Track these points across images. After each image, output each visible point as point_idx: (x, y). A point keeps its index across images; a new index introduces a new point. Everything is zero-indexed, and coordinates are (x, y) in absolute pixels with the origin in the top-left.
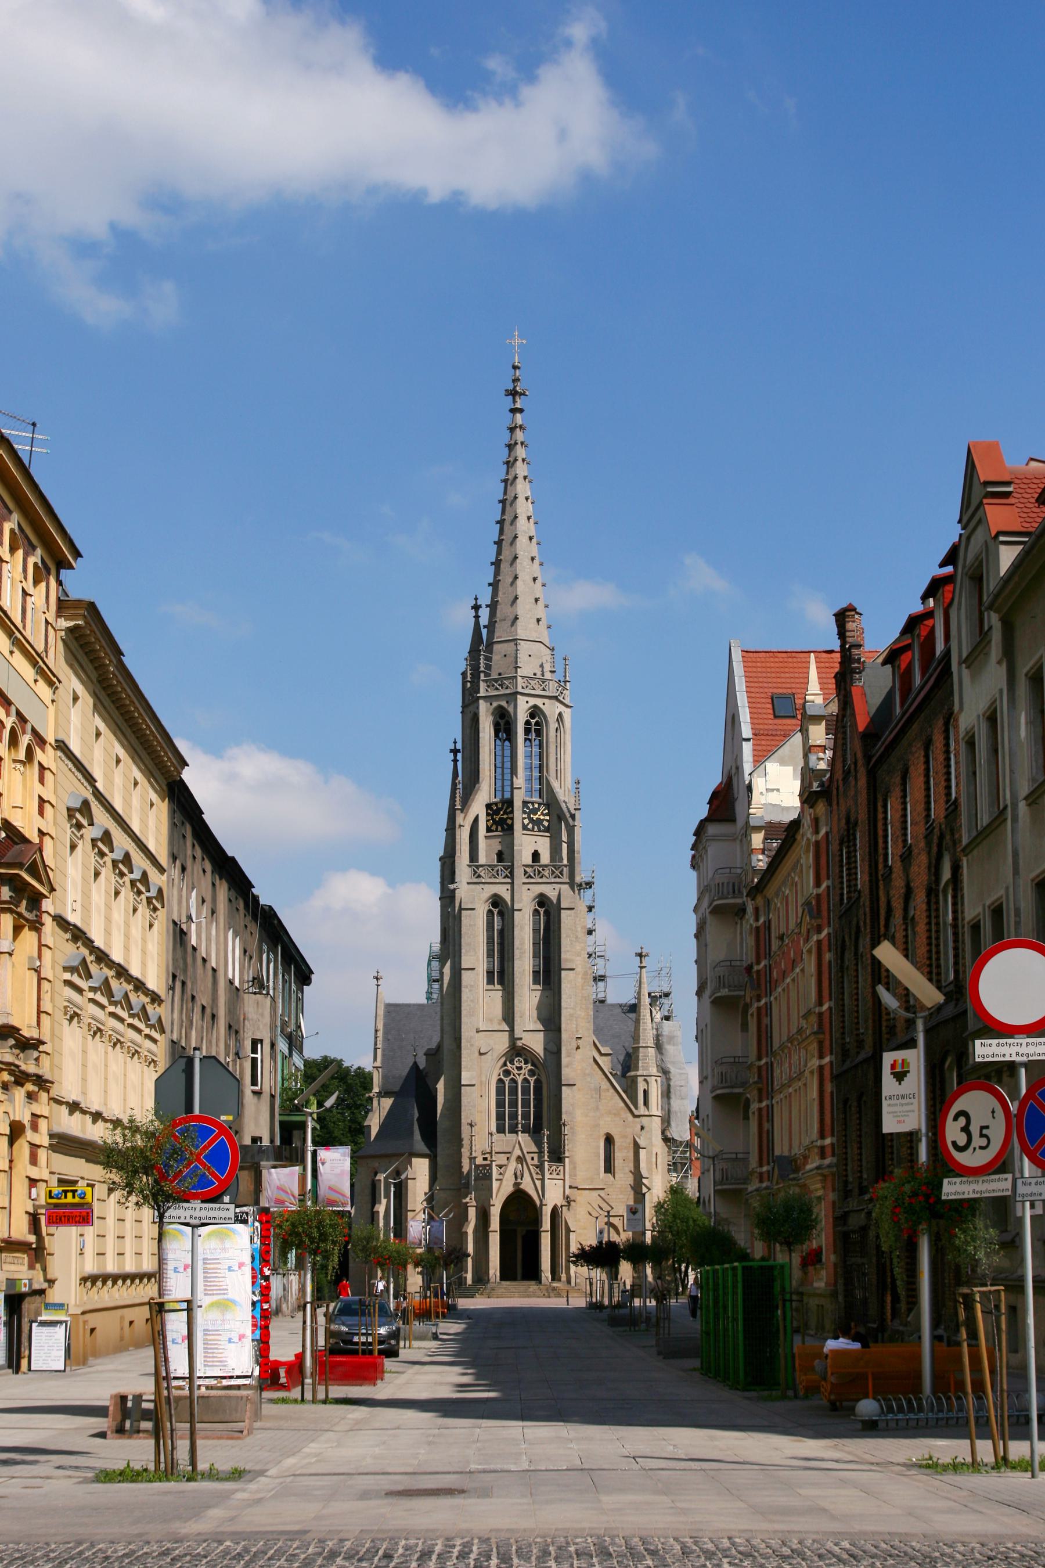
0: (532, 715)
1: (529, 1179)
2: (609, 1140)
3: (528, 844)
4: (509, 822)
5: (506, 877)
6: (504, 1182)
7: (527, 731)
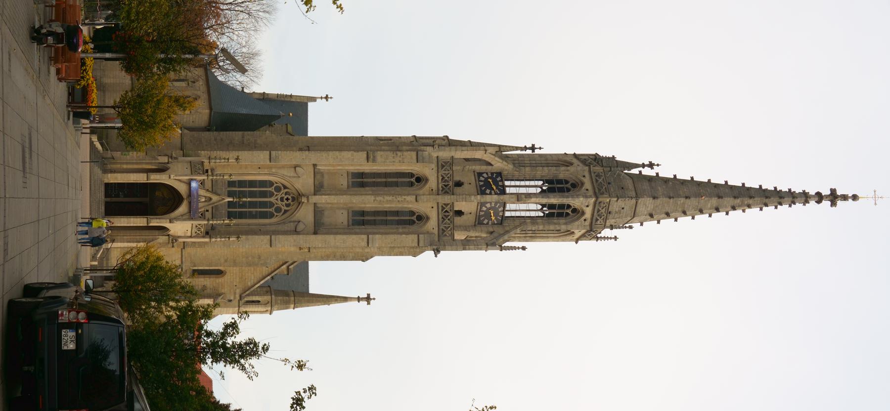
0: (575, 211)
2: (219, 273)
3: (468, 205)
4: (488, 191)
5: (443, 189)
7: (562, 206)
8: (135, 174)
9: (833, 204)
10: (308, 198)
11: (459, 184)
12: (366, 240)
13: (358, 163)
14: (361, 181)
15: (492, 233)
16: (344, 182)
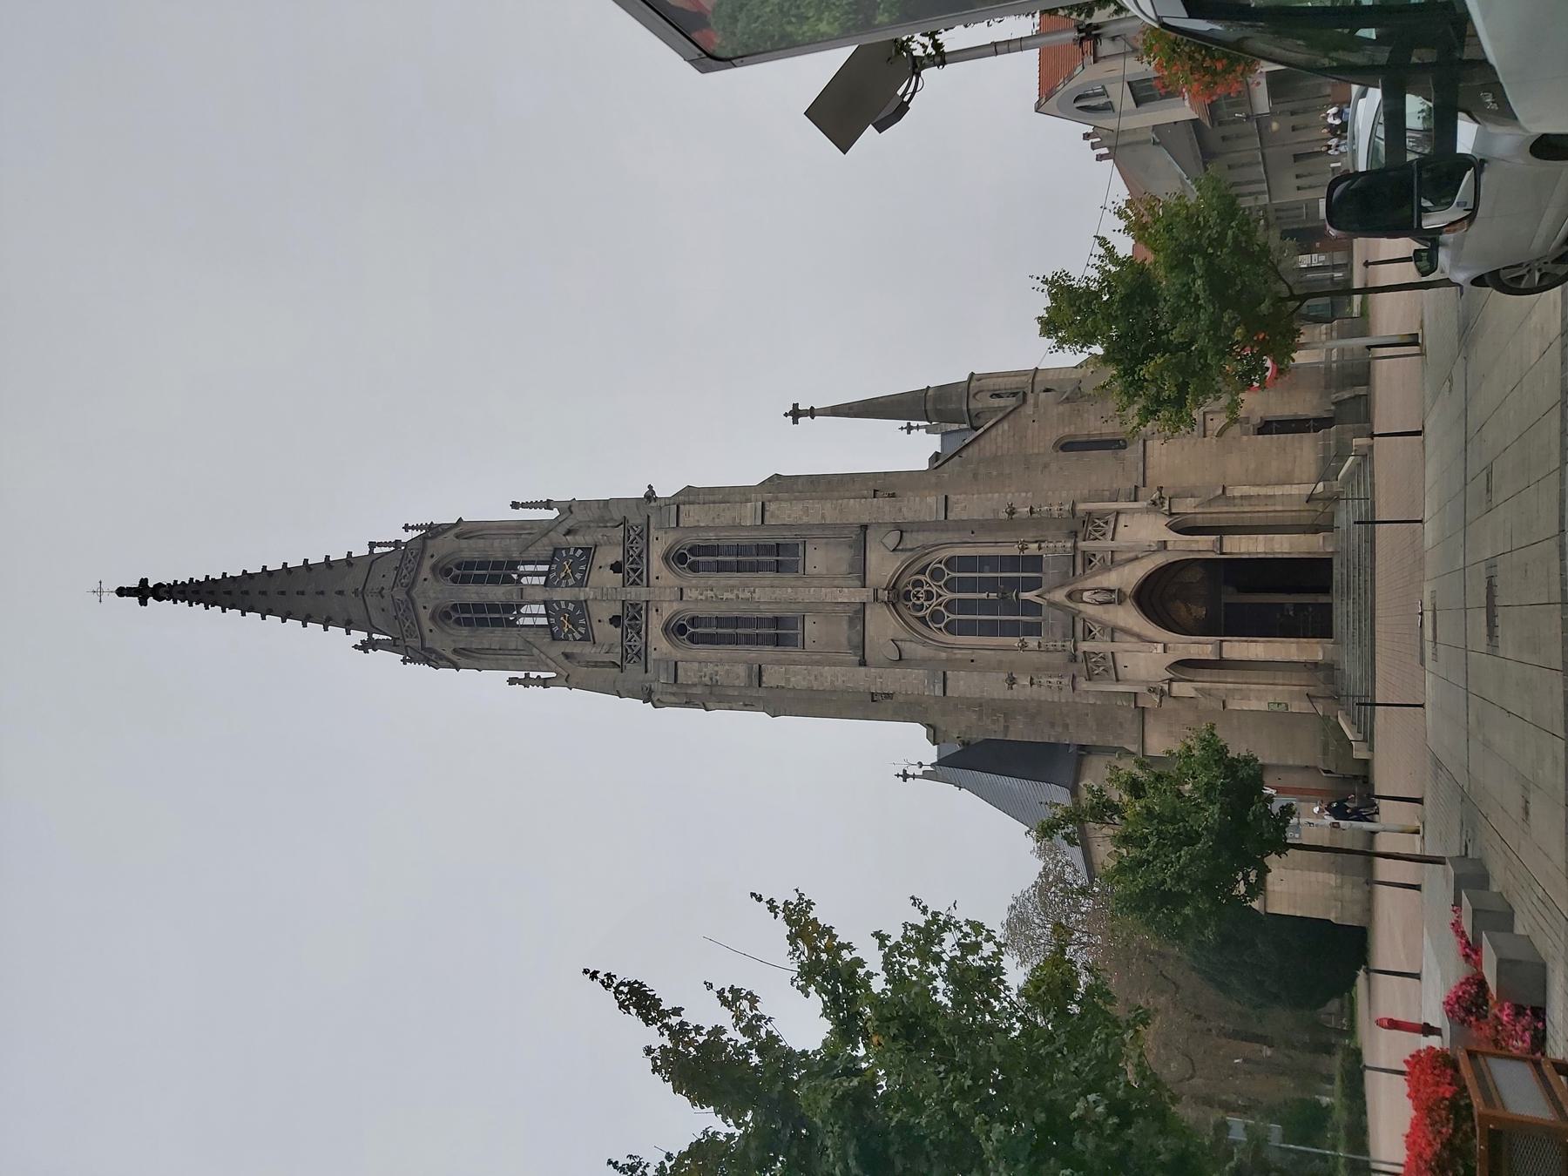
0: (447, 572)
2: (1067, 446)
4: (571, 607)
5: (639, 612)
6: (1121, 624)
7: (465, 580)
8: (1253, 658)
9: (144, 582)
10: (876, 599)
11: (615, 621)
12: (767, 514)
13: (780, 669)
14: (778, 631)
15: (569, 532)
16: (812, 629)
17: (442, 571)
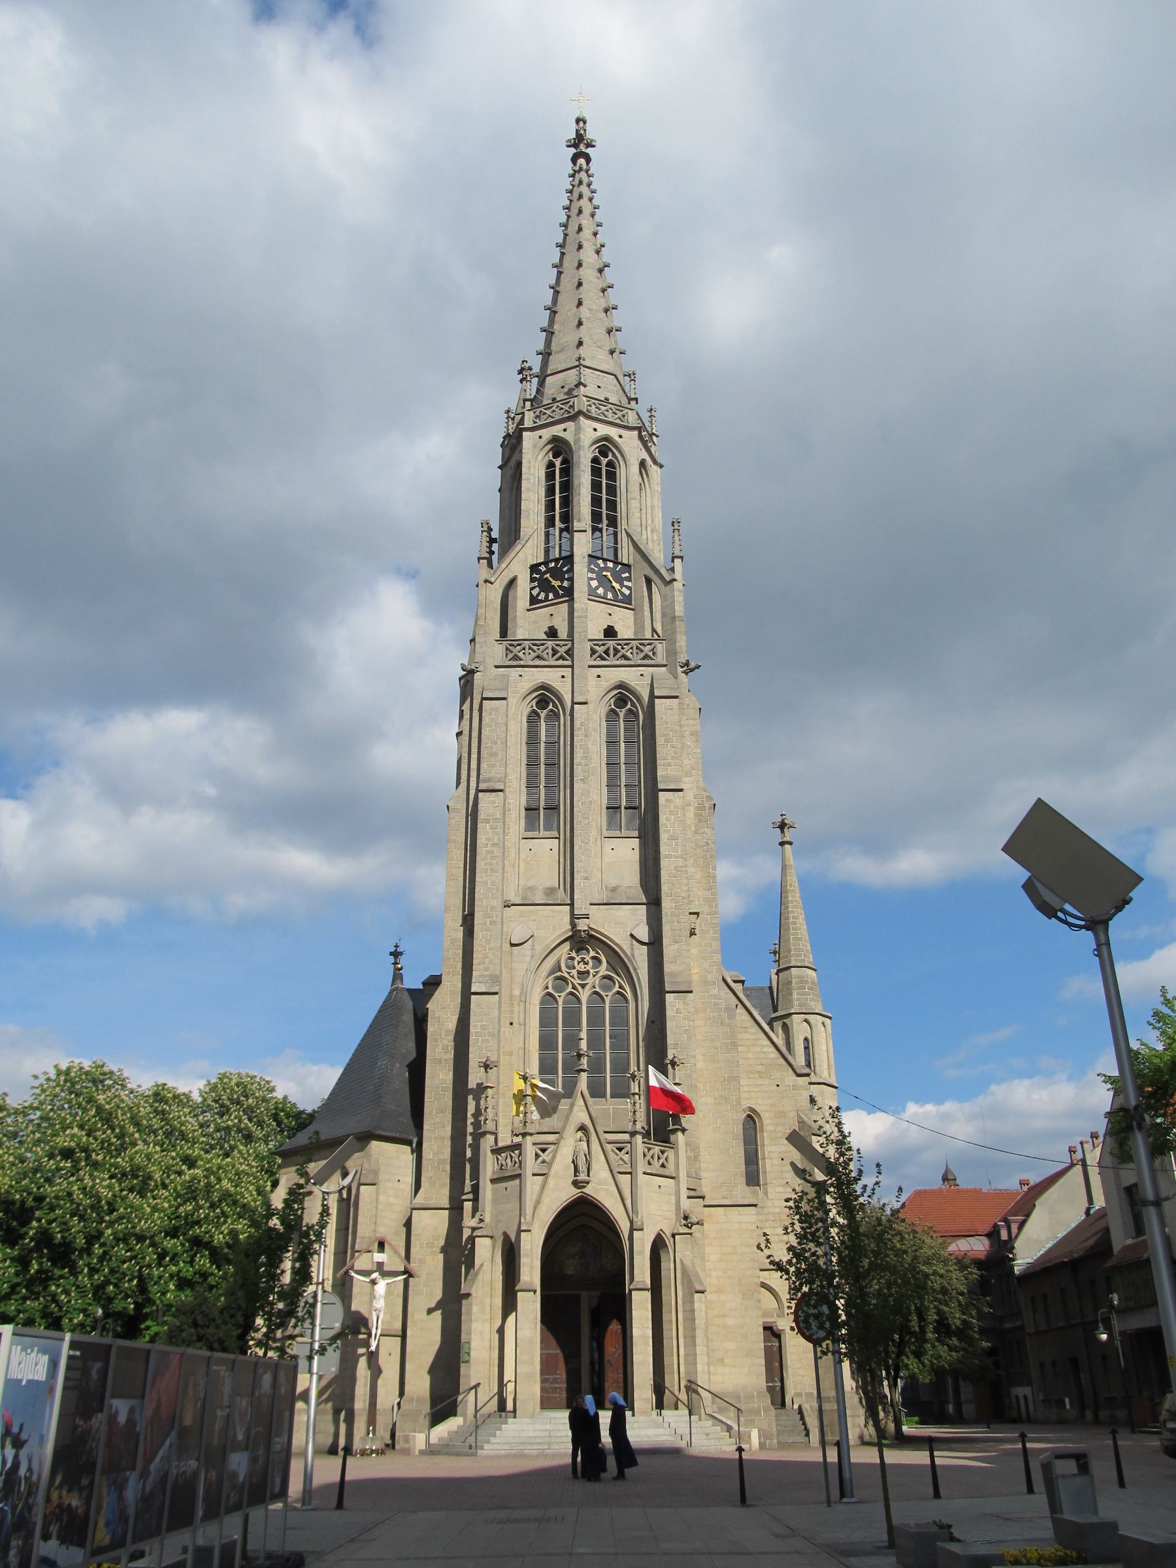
0: (604, 452)
1: (605, 1174)
2: (751, 1120)
4: (566, 584)
5: (562, 658)
6: (551, 1182)
7: (596, 472)
11: (552, 633)
15: (649, 581)
17: (605, 447)
